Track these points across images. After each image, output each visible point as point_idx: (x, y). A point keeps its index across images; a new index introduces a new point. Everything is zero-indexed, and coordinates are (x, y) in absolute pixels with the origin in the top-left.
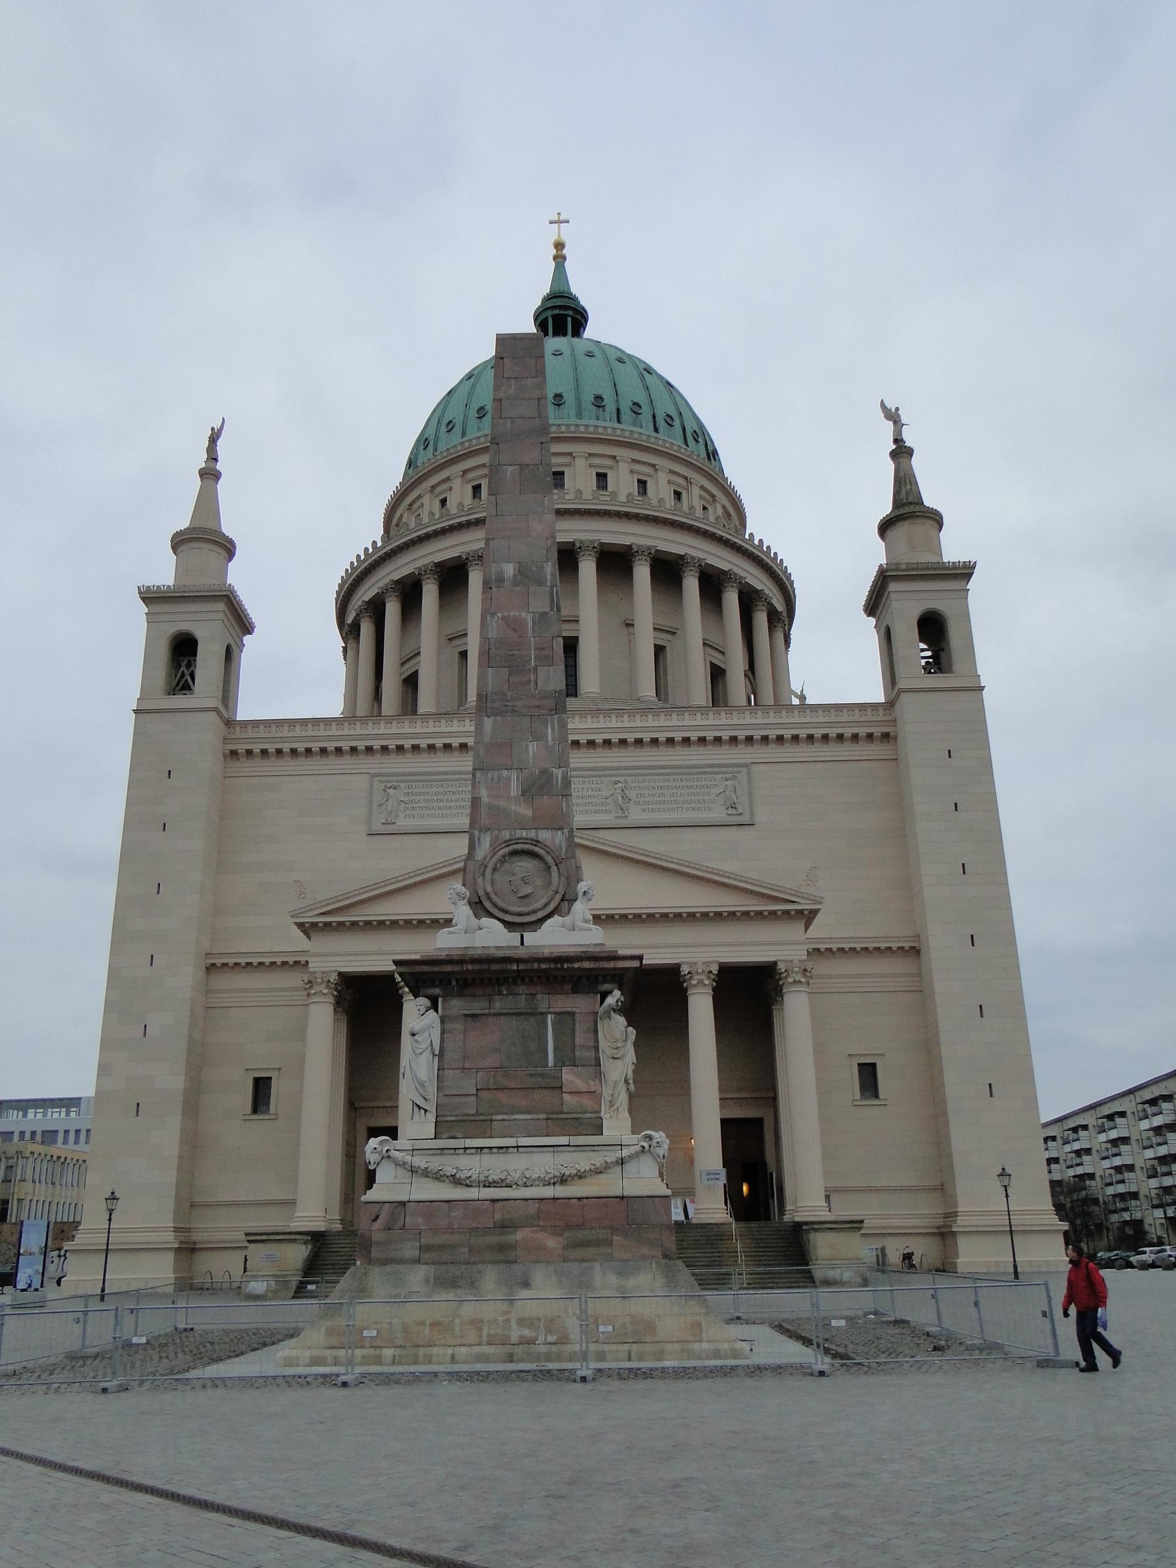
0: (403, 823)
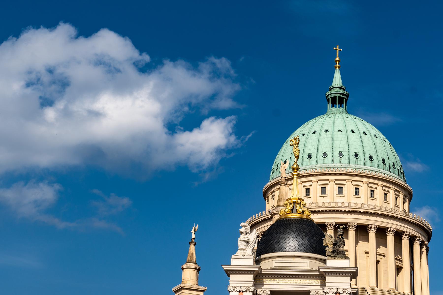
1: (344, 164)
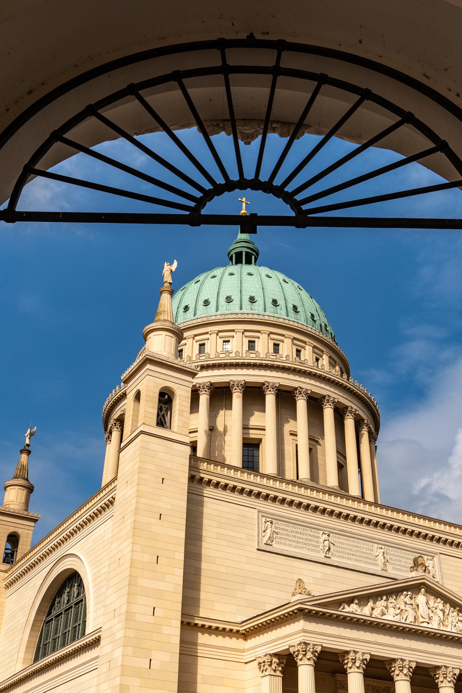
0: (276, 547)
1: (257, 312)
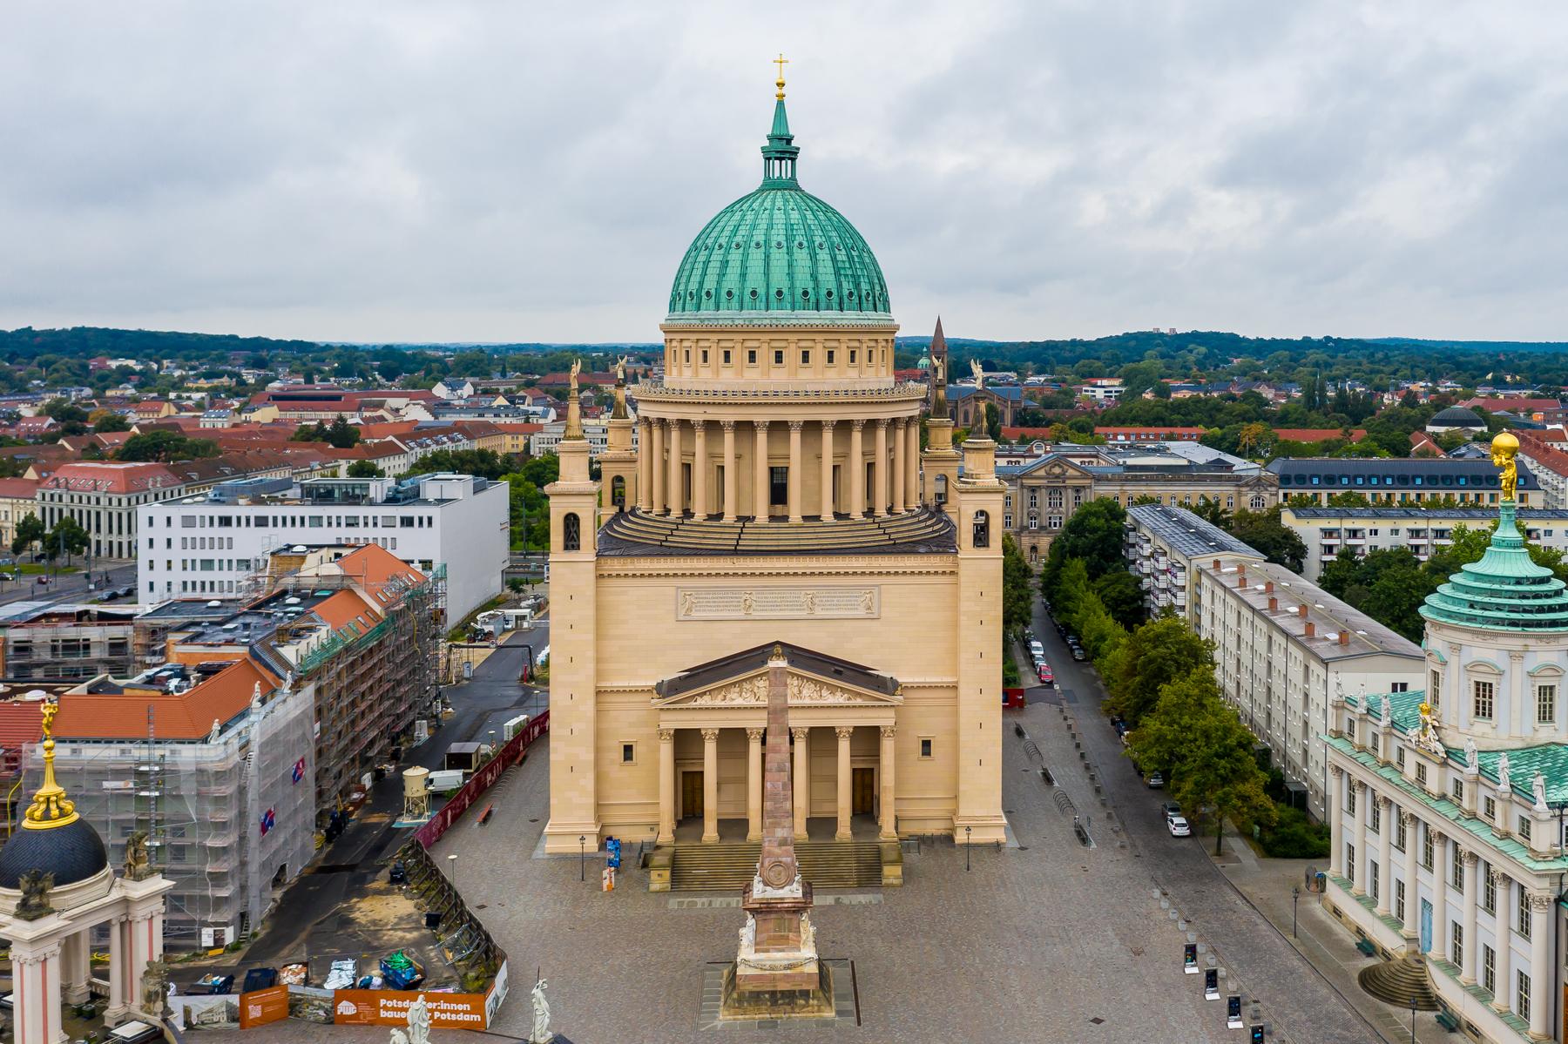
0: (695, 615)
